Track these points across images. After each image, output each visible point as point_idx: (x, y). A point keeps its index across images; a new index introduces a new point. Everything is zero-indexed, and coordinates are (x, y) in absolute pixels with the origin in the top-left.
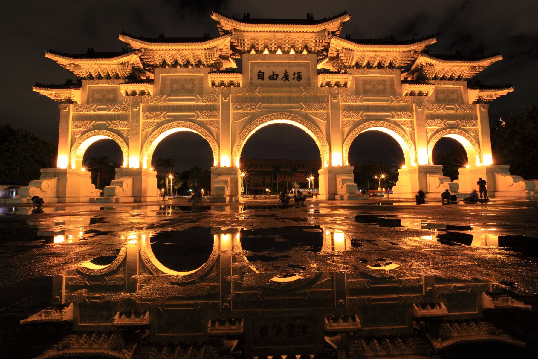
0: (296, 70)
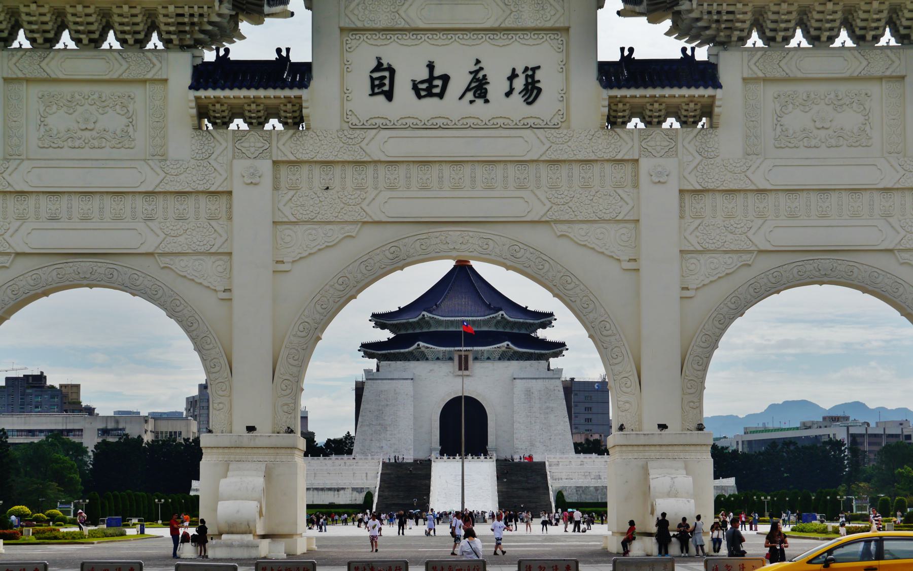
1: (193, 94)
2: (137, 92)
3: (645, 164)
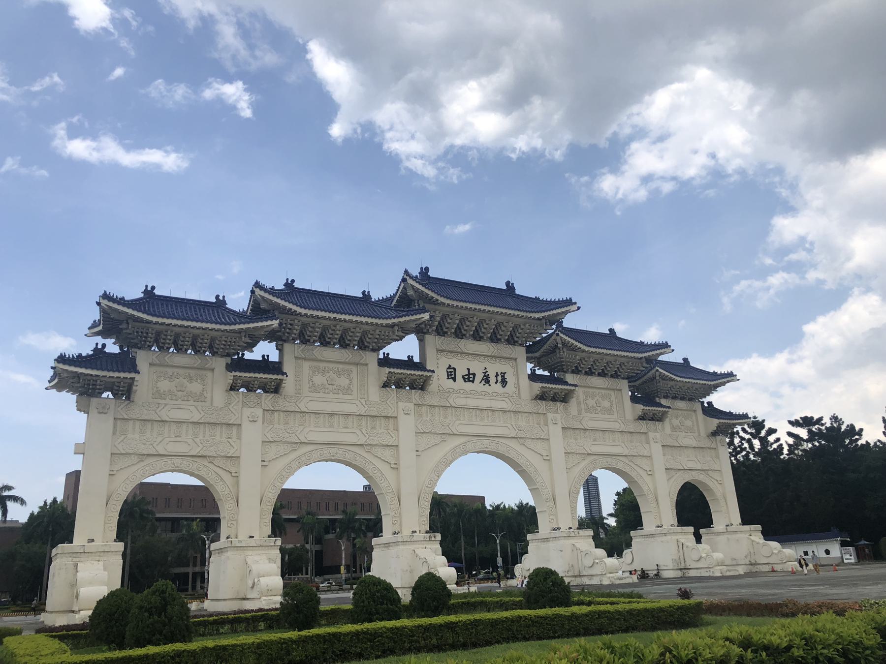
2: (354, 368)
3: (550, 416)
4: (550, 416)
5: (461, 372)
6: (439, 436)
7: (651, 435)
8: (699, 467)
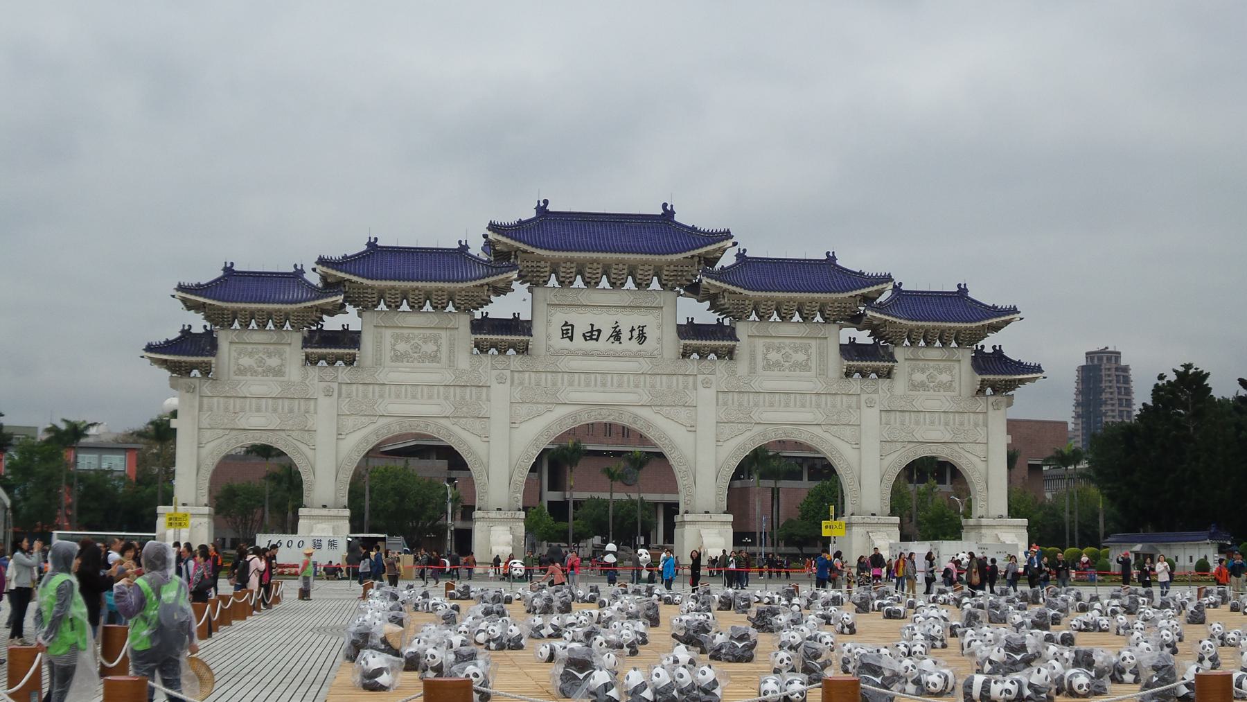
0: (636, 319)
1: (474, 337)
4: (700, 378)
5: (581, 328)
6: (543, 406)
7: (864, 397)
8: (948, 438)
